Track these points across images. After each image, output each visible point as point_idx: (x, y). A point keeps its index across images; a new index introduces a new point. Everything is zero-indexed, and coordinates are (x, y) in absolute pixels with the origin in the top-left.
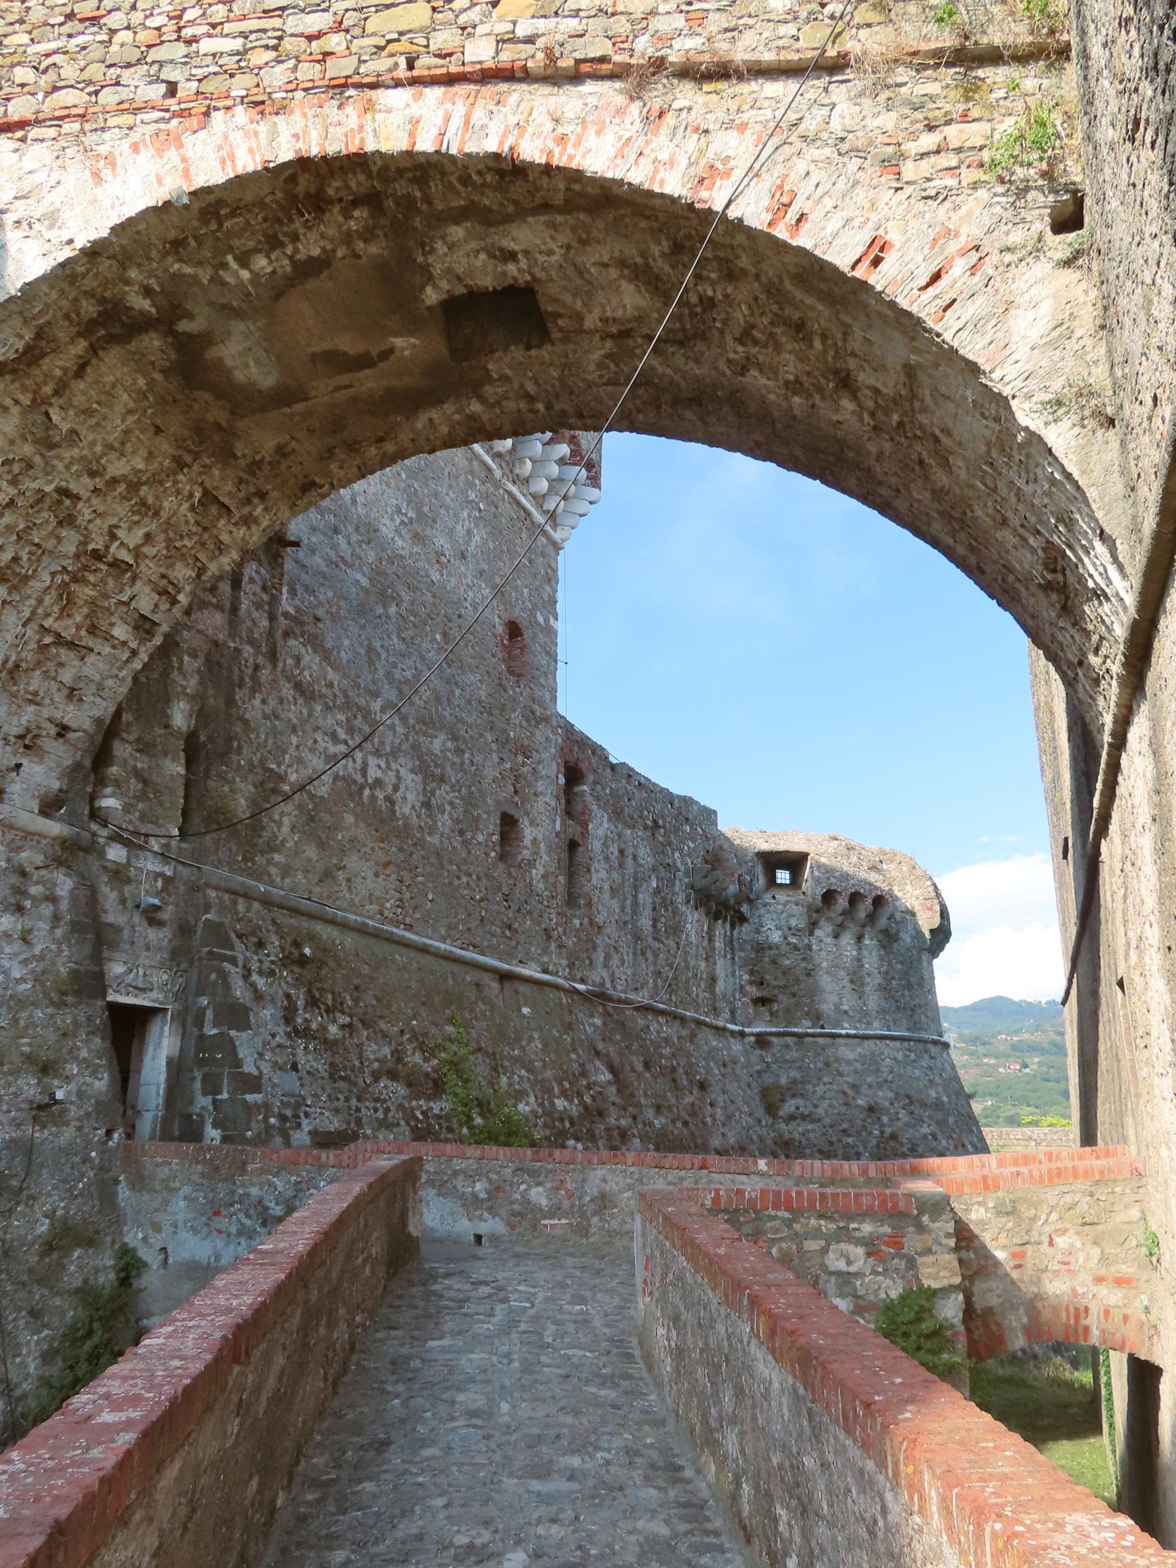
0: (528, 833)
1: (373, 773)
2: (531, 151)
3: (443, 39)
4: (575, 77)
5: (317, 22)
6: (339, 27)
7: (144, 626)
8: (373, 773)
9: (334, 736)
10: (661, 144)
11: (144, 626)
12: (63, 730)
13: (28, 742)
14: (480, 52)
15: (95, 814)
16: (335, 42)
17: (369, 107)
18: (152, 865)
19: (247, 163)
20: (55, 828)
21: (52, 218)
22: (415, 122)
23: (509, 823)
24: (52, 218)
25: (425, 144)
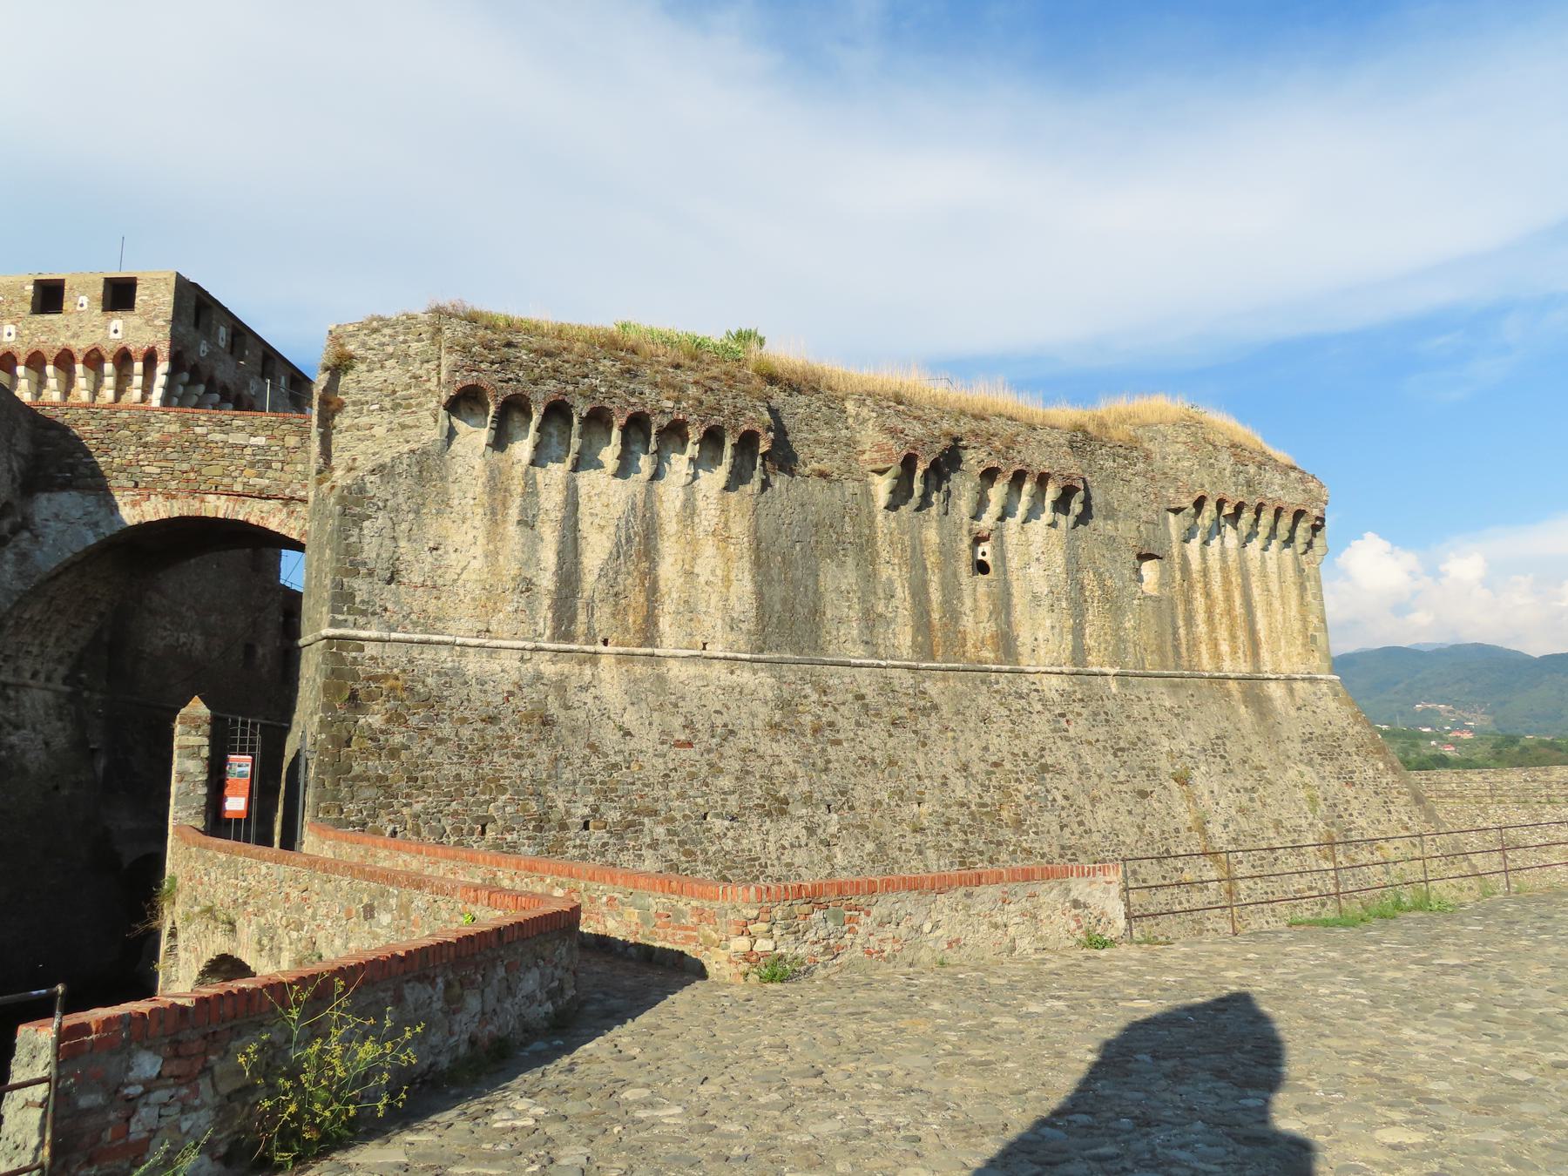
0: (260, 651)
1: (182, 640)
2: (253, 520)
3: (226, 481)
4: (268, 498)
5: (185, 466)
6: (192, 470)
7: (101, 615)
8: (182, 640)
9: (165, 629)
10: (292, 523)
11: (101, 615)
12: (71, 654)
13: (60, 661)
14: (238, 488)
15: (80, 681)
16: (192, 475)
17: (203, 501)
18: (97, 697)
19: (163, 515)
20: (67, 689)
21: (96, 524)
22: (217, 507)
23: (249, 650)
24: (96, 524)
25: (221, 515)
